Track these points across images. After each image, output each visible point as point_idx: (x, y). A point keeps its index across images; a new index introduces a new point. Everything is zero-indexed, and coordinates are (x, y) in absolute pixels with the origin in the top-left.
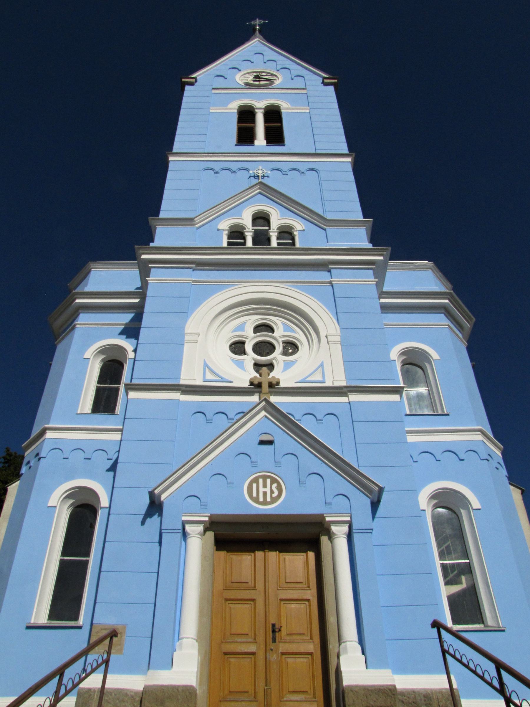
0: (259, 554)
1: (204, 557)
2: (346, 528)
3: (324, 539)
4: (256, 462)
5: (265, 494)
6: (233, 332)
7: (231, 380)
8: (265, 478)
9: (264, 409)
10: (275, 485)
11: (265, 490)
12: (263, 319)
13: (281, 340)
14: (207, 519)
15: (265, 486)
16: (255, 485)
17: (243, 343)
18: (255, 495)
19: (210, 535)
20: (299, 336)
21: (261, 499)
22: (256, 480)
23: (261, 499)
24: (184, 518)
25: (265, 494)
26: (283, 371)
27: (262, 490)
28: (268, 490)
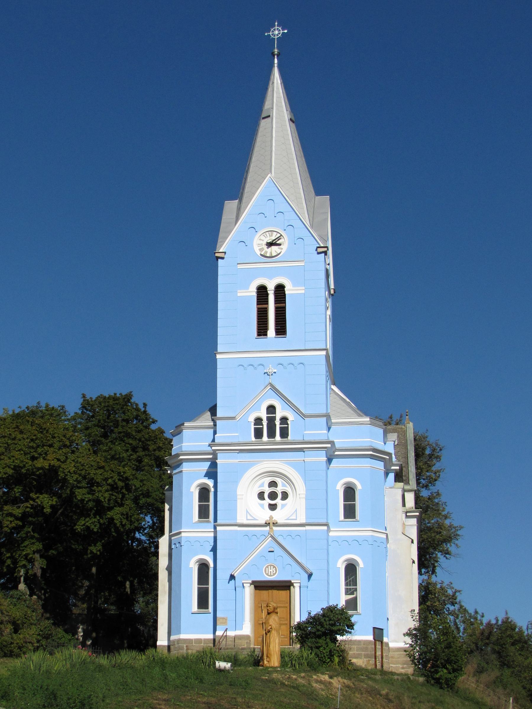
0: (270, 591)
1: (251, 594)
2: (299, 584)
3: (292, 587)
4: (267, 560)
5: (271, 572)
6: (259, 487)
7: (258, 519)
8: (271, 566)
9: (270, 537)
10: (274, 569)
11: (271, 570)
12: (272, 479)
13: (280, 492)
14: (251, 582)
15: (271, 569)
16: (267, 569)
17: (264, 492)
18: (267, 573)
19: (253, 586)
20: (288, 489)
21: (269, 574)
22: (267, 567)
23: (269, 574)
24: (243, 582)
25: (271, 572)
26: (281, 509)
27: (270, 570)
28: (272, 571)
